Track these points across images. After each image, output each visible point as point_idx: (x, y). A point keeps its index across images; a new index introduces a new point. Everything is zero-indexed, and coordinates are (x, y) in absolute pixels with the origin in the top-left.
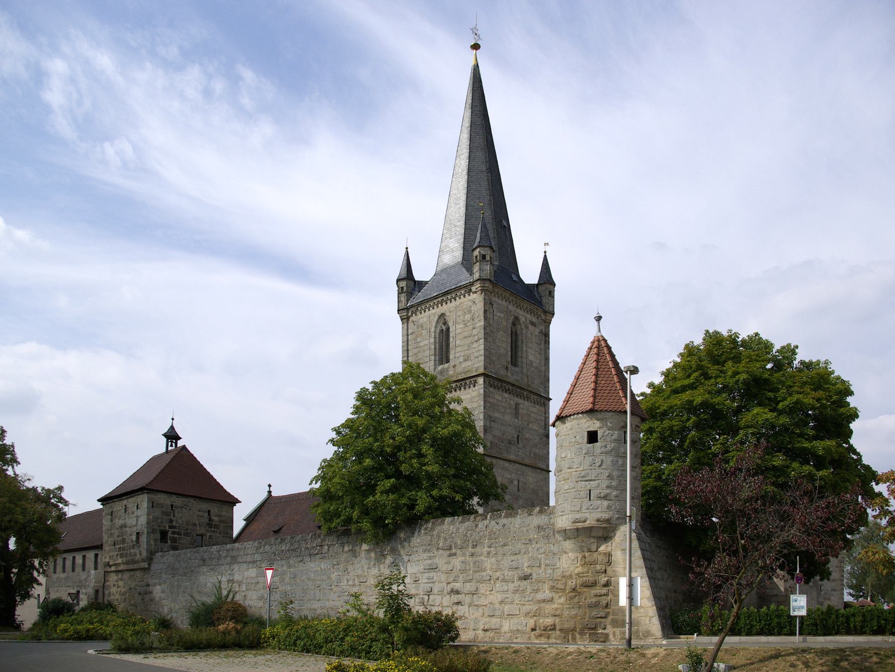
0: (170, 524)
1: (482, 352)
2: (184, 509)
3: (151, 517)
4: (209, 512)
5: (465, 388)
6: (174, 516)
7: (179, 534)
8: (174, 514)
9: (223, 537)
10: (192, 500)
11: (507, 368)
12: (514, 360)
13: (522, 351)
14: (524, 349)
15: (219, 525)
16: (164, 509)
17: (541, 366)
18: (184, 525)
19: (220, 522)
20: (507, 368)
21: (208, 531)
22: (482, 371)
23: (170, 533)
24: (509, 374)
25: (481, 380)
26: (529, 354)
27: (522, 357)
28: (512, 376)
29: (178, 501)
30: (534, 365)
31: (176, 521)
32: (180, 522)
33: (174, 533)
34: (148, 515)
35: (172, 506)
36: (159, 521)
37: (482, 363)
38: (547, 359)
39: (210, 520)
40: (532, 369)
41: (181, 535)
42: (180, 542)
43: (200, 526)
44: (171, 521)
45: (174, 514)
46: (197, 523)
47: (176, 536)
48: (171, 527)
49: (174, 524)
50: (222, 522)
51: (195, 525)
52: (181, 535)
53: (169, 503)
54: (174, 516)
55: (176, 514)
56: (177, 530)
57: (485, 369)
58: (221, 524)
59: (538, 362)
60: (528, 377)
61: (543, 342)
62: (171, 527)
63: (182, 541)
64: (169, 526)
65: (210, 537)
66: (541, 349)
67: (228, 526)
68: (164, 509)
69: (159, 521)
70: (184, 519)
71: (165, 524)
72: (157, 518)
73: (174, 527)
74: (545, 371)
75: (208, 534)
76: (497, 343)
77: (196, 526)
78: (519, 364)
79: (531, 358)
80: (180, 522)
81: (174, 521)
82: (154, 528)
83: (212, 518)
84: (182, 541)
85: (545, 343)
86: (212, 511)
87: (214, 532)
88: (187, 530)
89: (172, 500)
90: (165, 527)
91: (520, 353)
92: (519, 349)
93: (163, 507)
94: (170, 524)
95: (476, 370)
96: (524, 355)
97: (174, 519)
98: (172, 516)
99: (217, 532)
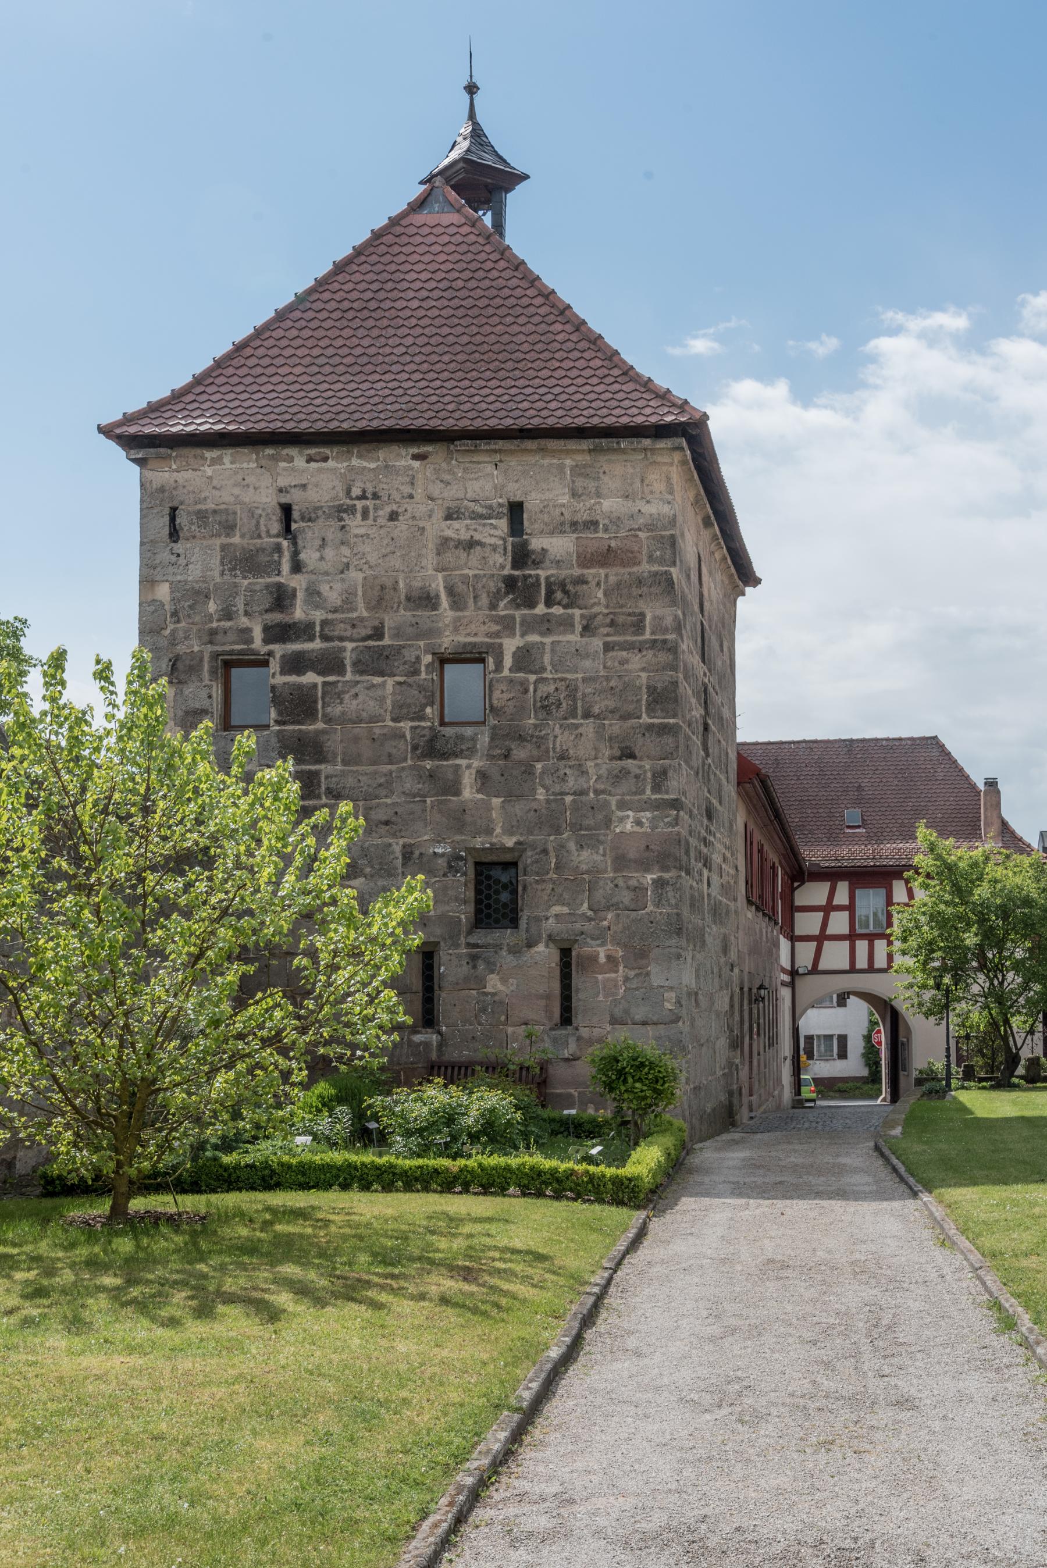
0: (277, 617)
3: (163, 592)
4: (516, 510)
6: (297, 567)
7: (330, 664)
8: (296, 553)
9: (608, 647)
10: (402, 458)
15: (582, 581)
16: (236, 540)
19: (587, 560)
21: (508, 626)
31: (313, 592)
32: (332, 594)
33: (295, 664)
34: (147, 582)
35: (287, 510)
36: (212, 607)
39: (522, 556)
41: (340, 670)
42: (336, 710)
43: (457, 602)
44: (281, 598)
45: (296, 553)
46: (438, 585)
47: (310, 678)
48: (279, 633)
49: (299, 614)
50: (606, 557)
51: (426, 600)
52: (340, 670)
53: (267, 499)
54: (297, 567)
55: (311, 556)
56: (317, 645)
58: (590, 572)
62: (279, 633)
63: (350, 705)
64: (266, 629)
65: (525, 659)
67: (640, 582)
68: (236, 540)
69: (212, 607)
70: (356, 576)
71: (244, 621)
72: (201, 595)
73: (305, 631)
75: (511, 645)
77: (435, 606)
80: (332, 594)
81: (300, 595)
82: (181, 649)
83: (536, 544)
84: (350, 705)
86: (533, 503)
87: (546, 625)
88: (378, 633)
89: (282, 482)
90: (245, 634)
93: (229, 528)
94: (277, 617)
97: (298, 583)
98: (286, 567)
99: (567, 624)
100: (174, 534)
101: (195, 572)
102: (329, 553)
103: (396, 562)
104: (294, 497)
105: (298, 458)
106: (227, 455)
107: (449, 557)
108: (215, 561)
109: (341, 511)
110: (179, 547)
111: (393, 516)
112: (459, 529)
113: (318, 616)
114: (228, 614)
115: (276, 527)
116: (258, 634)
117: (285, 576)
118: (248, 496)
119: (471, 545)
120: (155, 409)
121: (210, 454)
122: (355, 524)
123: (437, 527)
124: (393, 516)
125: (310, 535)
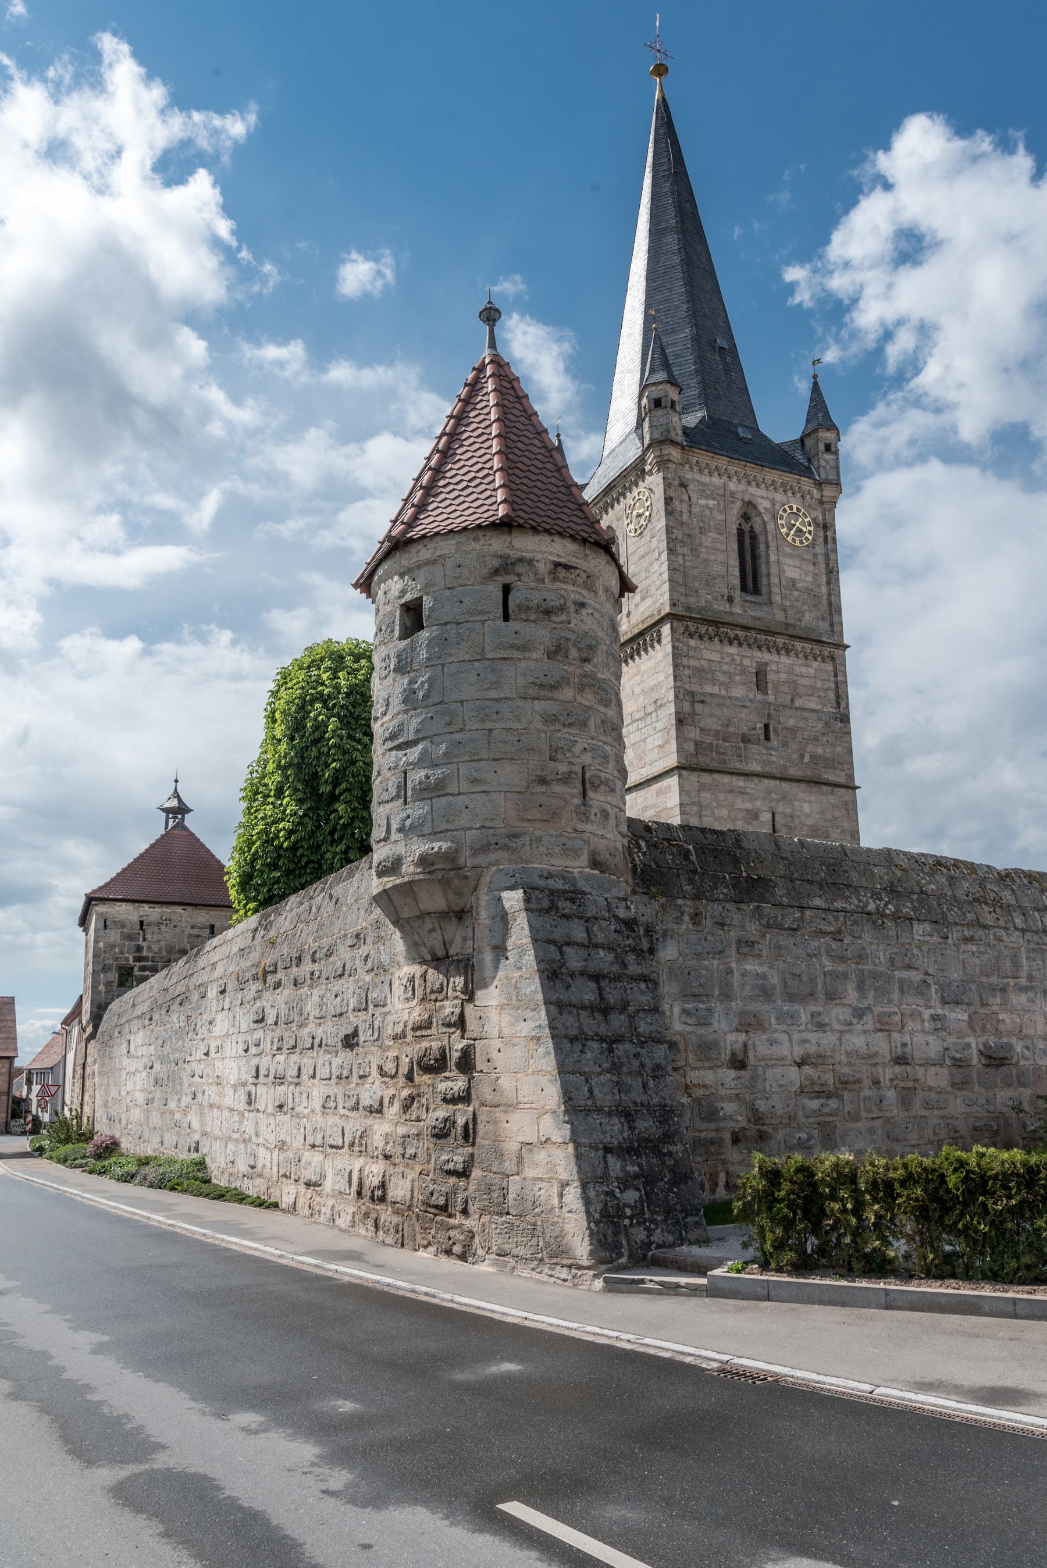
0: (138, 954)
1: (666, 576)
2: (163, 928)
3: (101, 945)
5: (646, 651)
6: (144, 940)
11: (730, 600)
12: (750, 583)
13: (768, 562)
14: (773, 558)
17: (819, 586)
18: (164, 954)
20: (730, 600)
22: (667, 609)
23: (136, 969)
24: (737, 610)
25: (666, 630)
26: (786, 567)
27: (768, 575)
28: (741, 610)
29: (153, 913)
30: (800, 585)
31: (149, 948)
32: (155, 948)
35: (142, 923)
37: (667, 597)
38: (831, 572)
40: (796, 593)
44: (139, 949)
48: (137, 959)
49: (145, 953)
53: (135, 918)
54: (144, 940)
55: (149, 937)
56: (150, 963)
57: (673, 604)
59: (809, 579)
60: (785, 611)
61: (821, 540)
66: (815, 555)
69: (117, 950)
70: (163, 943)
71: (127, 955)
73: (146, 959)
74: (829, 595)
76: (703, 555)
78: (764, 589)
79: (792, 573)
80: (155, 948)
85: (826, 542)
91: (763, 568)
92: (763, 560)
93: (123, 926)
94: (138, 954)
95: (659, 612)
96: (774, 570)
97: (145, 944)
98: (141, 939)
100: (105, 927)
101: (111, 939)
102: (155, 936)
103: (175, 940)
104: (145, 919)
105: (146, 907)
106: (124, 904)
107: (192, 939)
108: (118, 936)
109: (159, 924)
110: (107, 931)
111: (175, 926)
112: (195, 932)
113: (150, 955)
114: (122, 953)
115: (138, 927)
116: (131, 959)
117: (141, 942)
118: (130, 917)
119: (198, 936)
120: (100, 889)
121: (118, 904)
122: (163, 928)
123: (188, 930)
124: (175, 926)
125: (149, 930)
